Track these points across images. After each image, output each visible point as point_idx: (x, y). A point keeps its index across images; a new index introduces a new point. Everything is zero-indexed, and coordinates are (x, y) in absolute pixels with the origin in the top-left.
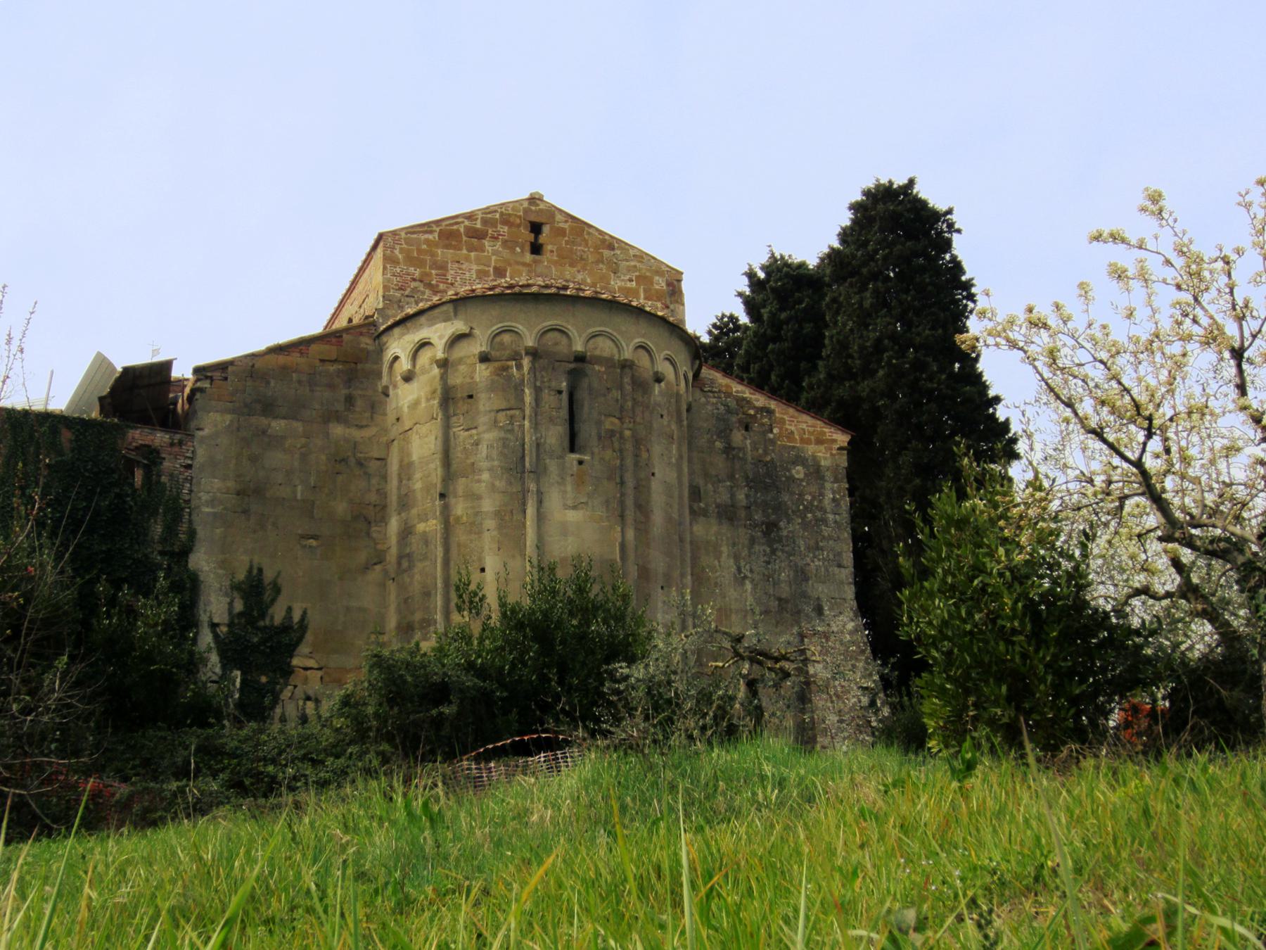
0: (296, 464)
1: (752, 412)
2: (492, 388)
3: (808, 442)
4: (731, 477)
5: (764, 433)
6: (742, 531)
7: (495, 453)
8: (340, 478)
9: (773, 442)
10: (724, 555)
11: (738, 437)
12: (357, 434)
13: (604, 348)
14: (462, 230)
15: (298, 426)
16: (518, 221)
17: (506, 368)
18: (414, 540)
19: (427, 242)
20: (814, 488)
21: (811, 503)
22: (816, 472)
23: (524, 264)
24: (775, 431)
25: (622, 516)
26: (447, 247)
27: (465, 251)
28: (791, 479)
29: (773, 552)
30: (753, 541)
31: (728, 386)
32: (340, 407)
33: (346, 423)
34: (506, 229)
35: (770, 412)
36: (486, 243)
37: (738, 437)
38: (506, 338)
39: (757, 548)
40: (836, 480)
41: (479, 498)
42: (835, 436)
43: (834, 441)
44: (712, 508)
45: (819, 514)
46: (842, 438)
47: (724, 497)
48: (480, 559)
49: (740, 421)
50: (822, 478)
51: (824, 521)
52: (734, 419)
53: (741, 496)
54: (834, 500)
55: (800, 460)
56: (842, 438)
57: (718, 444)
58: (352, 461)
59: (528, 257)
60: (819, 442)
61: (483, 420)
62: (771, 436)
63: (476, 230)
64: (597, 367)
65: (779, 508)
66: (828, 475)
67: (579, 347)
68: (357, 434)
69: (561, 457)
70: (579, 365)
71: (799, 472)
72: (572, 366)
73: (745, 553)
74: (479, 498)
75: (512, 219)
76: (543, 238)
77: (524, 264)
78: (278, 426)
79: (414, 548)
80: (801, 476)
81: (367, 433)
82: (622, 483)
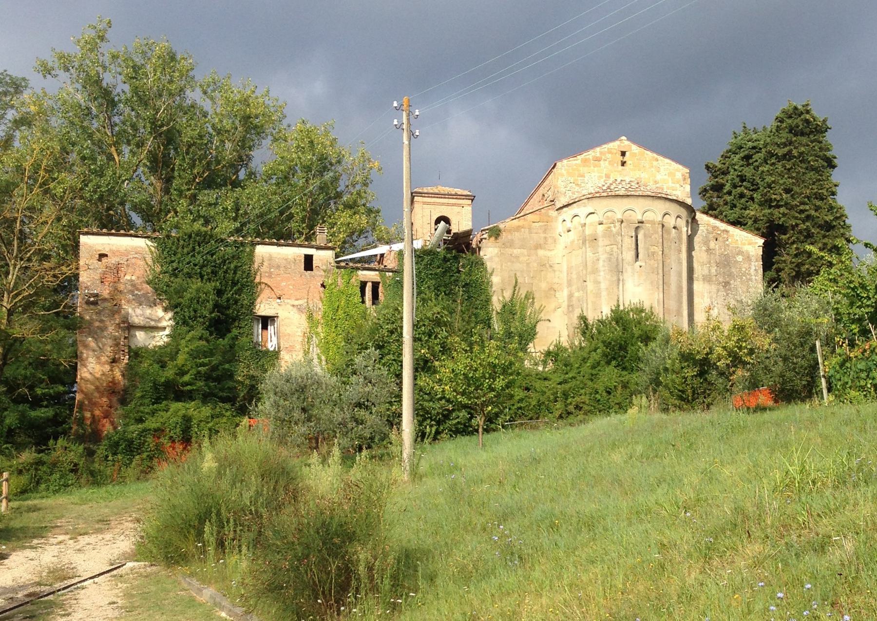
0: (525, 268)
1: (719, 232)
2: (604, 236)
3: (744, 244)
4: (710, 262)
5: (724, 242)
6: (713, 286)
7: (606, 264)
8: (543, 273)
9: (728, 245)
10: (706, 298)
11: (712, 244)
12: (549, 254)
13: (649, 216)
14: (591, 158)
15: (525, 251)
16: (615, 151)
17: (609, 228)
18: (574, 299)
19: (576, 165)
20: (746, 265)
21: (745, 272)
22: (748, 258)
23: (618, 172)
24: (730, 240)
25: (658, 288)
26: (584, 166)
27: (592, 168)
28: (736, 262)
29: (727, 295)
30: (718, 291)
31: (708, 221)
32: (542, 242)
33: (545, 249)
34: (610, 155)
35: (727, 231)
36: (602, 162)
37: (712, 244)
38: (609, 214)
39: (720, 293)
40: (757, 261)
41: (600, 283)
42: (757, 241)
43: (757, 243)
44: (701, 277)
45: (748, 277)
46: (761, 241)
47: (706, 272)
48: (601, 308)
49: (714, 237)
50: (751, 260)
51: (750, 280)
52: (711, 236)
53: (713, 270)
54: (755, 270)
55: (740, 253)
56: (761, 241)
57: (704, 248)
58: (548, 265)
59: (620, 168)
60: (750, 244)
61: (600, 249)
62: (727, 243)
63: (597, 157)
64: (647, 225)
65: (731, 275)
66: (753, 259)
67: (639, 218)
68: (549, 254)
69: (633, 265)
70: (640, 224)
71: (740, 258)
72: (637, 225)
73: (714, 296)
74: (600, 283)
75: (613, 151)
76: (627, 158)
77: (618, 172)
78: (516, 251)
79: (574, 302)
80: (741, 260)
81: (553, 253)
82: (658, 274)
